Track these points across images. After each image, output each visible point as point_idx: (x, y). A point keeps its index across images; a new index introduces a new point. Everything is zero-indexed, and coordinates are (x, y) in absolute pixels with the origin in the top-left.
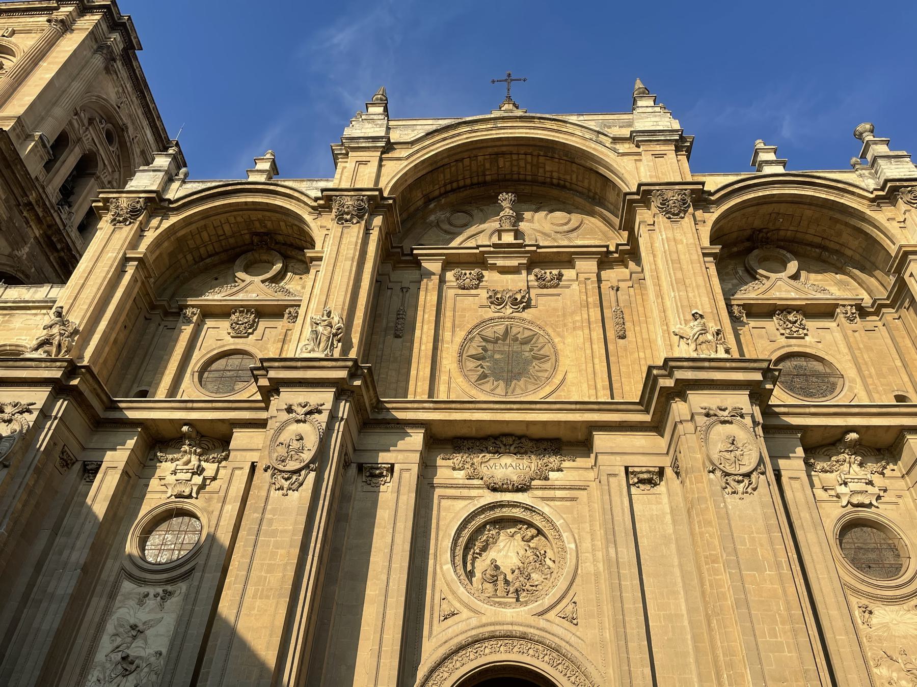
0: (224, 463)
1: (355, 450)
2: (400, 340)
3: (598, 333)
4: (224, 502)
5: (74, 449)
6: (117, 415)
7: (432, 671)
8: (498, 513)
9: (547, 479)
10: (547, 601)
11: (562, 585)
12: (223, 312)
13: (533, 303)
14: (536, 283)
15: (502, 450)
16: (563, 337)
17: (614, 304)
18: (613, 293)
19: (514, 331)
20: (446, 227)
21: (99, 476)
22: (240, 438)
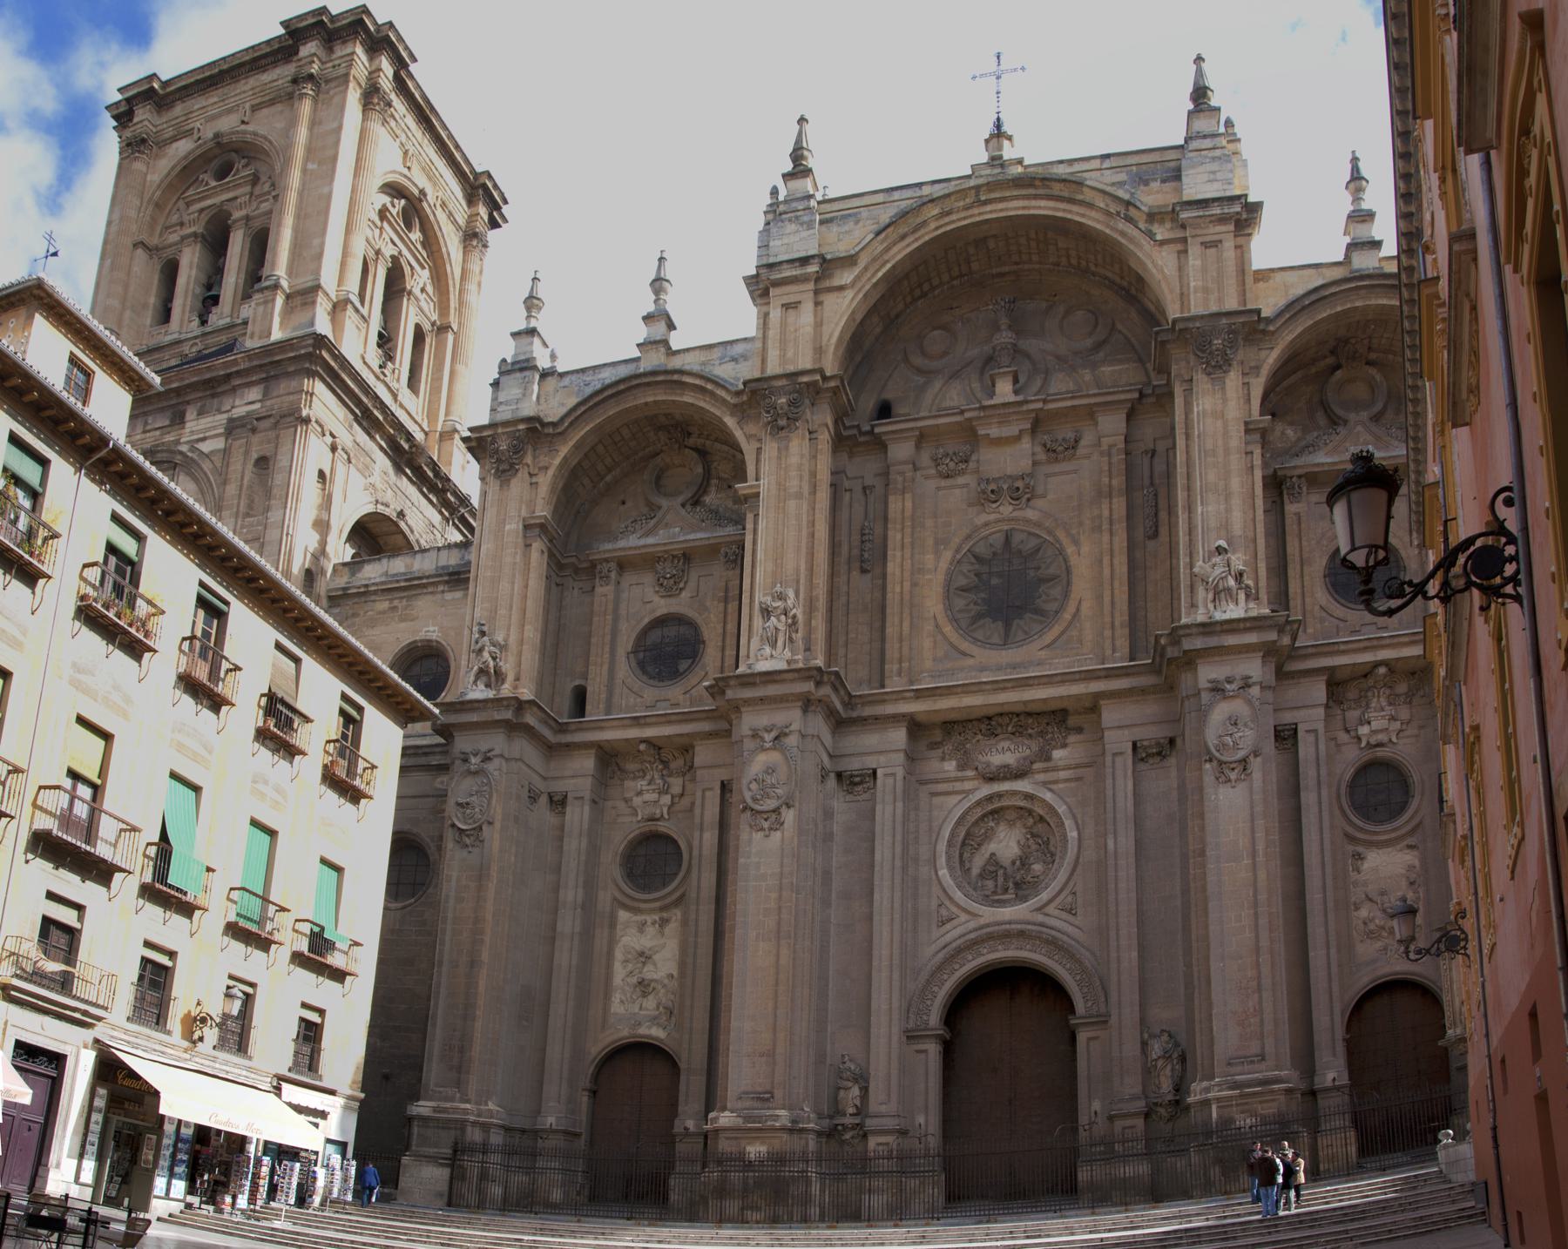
0: (688, 777)
1: (831, 756)
2: (869, 576)
3: (1120, 540)
4: (702, 830)
5: (539, 784)
6: (568, 738)
7: (933, 975)
8: (997, 805)
9: (1049, 759)
10: (1045, 896)
11: (1062, 876)
12: (648, 561)
13: (1040, 490)
14: (1042, 456)
15: (999, 730)
16: (1076, 542)
17: (1147, 481)
18: (1146, 460)
19: (1017, 539)
20: (918, 360)
21: (568, 809)
22: (704, 754)
